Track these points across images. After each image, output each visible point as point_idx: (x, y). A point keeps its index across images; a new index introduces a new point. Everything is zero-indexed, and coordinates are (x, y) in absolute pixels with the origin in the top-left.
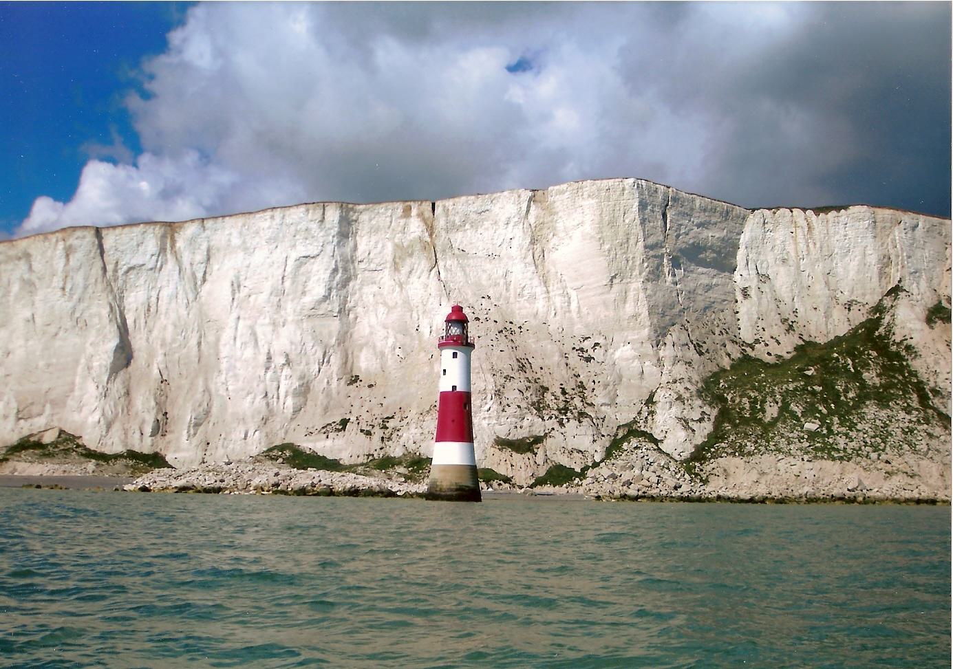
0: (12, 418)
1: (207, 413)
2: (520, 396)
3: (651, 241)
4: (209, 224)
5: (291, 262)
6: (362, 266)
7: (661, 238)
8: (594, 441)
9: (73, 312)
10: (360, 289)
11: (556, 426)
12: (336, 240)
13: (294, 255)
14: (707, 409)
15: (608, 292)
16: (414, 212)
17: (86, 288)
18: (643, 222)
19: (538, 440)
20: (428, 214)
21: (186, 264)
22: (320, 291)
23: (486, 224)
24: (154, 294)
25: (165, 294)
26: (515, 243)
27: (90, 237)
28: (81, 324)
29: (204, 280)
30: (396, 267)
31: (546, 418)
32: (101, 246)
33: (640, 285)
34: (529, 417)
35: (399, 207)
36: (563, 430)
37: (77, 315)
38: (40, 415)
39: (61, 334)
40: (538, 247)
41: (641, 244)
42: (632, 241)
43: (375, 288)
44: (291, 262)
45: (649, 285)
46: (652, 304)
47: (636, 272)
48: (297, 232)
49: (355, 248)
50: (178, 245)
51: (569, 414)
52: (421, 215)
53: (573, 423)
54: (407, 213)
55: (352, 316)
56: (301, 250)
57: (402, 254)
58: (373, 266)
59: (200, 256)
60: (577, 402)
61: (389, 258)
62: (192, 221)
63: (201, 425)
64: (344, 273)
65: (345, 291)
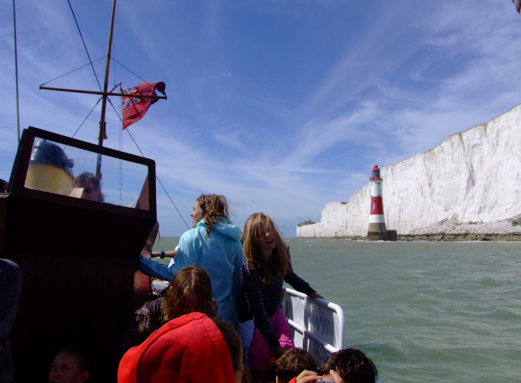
0: (444, 211)
1: (496, 203)
4: (496, 120)
17: (459, 157)
21: (490, 140)
24: (481, 155)
25: (485, 153)
27: (457, 137)
28: (458, 172)
29: (497, 145)
32: (461, 139)
38: (450, 209)
39: (454, 177)
50: (488, 132)
62: (490, 120)
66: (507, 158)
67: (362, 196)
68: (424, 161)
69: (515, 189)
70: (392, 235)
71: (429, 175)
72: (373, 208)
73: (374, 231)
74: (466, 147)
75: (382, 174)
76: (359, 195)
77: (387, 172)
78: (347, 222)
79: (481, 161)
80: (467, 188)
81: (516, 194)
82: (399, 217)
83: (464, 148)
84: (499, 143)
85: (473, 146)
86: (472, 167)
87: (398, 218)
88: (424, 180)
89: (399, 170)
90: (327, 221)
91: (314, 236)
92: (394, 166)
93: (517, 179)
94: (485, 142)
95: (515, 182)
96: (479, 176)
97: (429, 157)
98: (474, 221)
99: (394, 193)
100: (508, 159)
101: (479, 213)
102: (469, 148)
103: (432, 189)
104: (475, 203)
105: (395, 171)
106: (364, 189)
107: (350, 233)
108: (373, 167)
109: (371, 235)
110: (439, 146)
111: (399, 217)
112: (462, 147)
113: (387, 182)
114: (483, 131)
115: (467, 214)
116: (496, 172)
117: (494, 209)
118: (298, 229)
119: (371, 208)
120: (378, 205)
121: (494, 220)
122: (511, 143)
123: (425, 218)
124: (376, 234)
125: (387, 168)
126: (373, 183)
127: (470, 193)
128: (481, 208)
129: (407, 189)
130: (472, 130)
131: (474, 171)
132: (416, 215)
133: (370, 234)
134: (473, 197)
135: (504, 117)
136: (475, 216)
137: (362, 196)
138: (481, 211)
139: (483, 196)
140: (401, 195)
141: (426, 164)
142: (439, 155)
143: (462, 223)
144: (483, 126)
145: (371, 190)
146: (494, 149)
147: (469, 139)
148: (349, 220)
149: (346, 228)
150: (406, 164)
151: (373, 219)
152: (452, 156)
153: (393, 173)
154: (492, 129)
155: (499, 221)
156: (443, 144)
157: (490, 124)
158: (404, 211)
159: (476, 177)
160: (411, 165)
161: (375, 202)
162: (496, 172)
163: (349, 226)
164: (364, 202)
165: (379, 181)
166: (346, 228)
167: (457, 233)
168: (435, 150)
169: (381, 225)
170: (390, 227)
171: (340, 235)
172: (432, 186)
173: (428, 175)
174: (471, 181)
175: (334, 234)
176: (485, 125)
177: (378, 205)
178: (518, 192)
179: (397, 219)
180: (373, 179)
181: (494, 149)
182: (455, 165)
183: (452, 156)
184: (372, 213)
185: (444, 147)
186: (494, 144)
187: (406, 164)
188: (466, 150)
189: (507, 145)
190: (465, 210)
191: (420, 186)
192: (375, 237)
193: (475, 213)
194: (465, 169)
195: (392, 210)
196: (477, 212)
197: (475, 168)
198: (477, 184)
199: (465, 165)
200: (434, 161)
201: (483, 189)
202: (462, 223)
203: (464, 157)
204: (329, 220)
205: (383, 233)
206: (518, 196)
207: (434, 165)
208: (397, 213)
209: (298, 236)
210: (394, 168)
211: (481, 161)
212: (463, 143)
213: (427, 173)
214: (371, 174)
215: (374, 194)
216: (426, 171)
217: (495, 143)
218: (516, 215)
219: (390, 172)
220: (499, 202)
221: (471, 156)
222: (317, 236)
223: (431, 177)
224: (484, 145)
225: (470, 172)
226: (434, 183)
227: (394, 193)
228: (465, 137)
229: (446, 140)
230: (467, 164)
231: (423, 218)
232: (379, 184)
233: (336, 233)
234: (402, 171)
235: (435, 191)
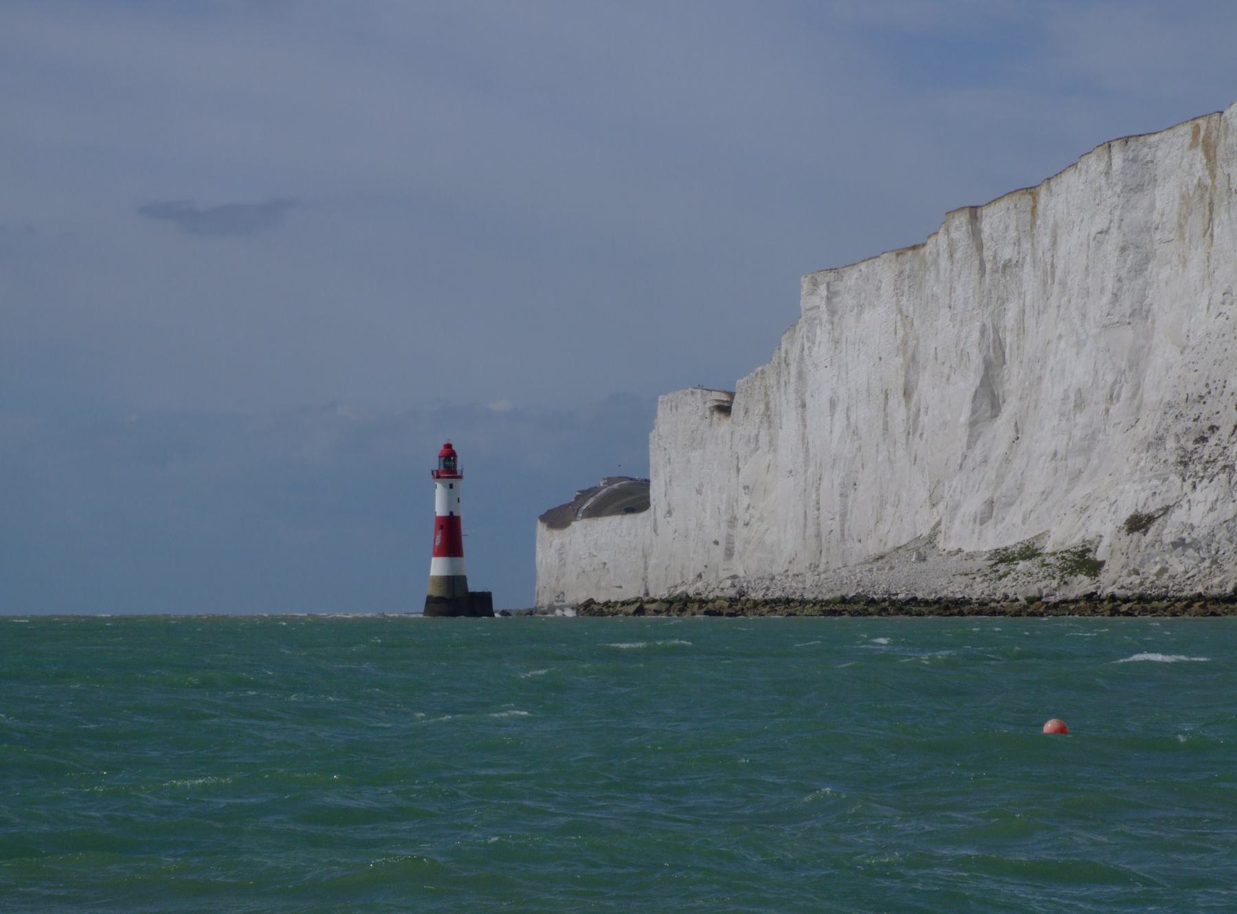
9: (957, 345)
27: (962, 219)
32: (976, 234)
35: (1188, 128)
49: (1152, 208)
63: (1011, 505)
65: (1141, 281)
70: (480, 604)
72: (437, 543)
74: (989, 266)
78: (732, 522)
79: (1021, 329)
80: (973, 424)
82: (844, 516)
86: (999, 345)
99: (833, 404)
103: (913, 409)
108: (442, 448)
111: (844, 516)
112: (977, 263)
113: (816, 349)
114: (1028, 217)
118: (550, 547)
127: (979, 443)
128: (991, 503)
131: (1004, 363)
133: (431, 601)
138: (991, 517)
141: (904, 300)
144: (1029, 197)
149: (729, 553)
151: (438, 567)
153: (833, 312)
159: (1007, 386)
161: (442, 528)
170: (474, 586)
172: (915, 398)
177: (450, 536)
180: (438, 477)
188: (987, 277)
193: (975, 521)
205: (459, 600)
209: (544, 600)
210: (839, 286)
212: (980, 247)
213: (905, 343)
214: (435, 464)
215: (440, 510)
216: (901, 333)
230: (983, 331)
232: (451, 486)
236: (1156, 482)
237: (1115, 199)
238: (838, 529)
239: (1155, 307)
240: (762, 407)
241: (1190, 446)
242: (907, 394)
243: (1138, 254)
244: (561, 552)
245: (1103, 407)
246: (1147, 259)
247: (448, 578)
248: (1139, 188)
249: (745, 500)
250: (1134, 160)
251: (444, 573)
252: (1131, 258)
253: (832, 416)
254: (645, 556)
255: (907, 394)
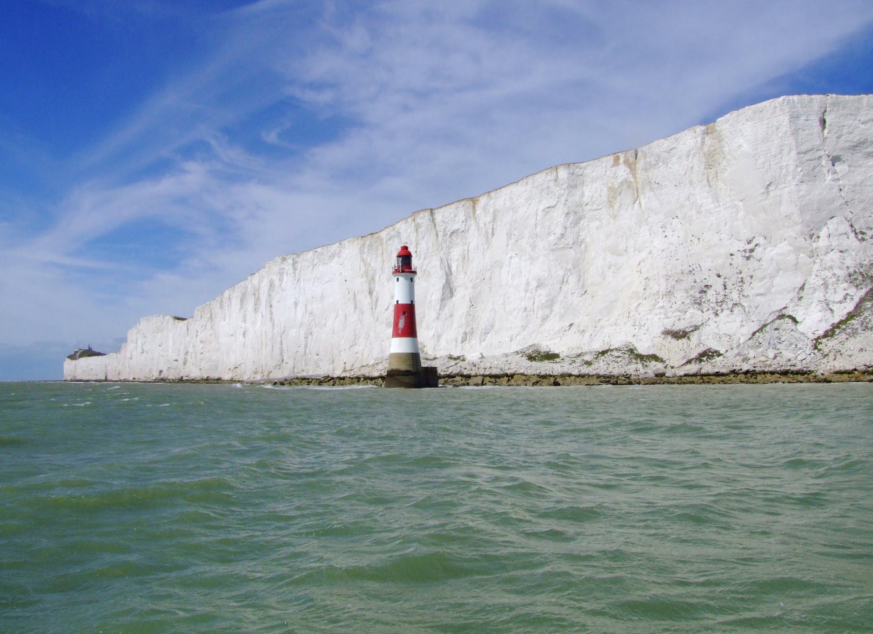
1: (492, 326)
2: (685, 295)
3: (804, 148)
4: (493, 194)
5: (540, 213)
6: (588, 207)
7: (818, 142)
8: (742, 326)
10: (588, 225)
11: (712, 316)
12: (567, 192)
13: (542, 207)
14: (852, 291)
15: (766, 199)
16: (622, 160)
17: (428, 249)
18: (795, 132)
19: (696, 328)
20: (631, 159)
21: (482, 225)
22: (559, 231)
23: (674, 159)
24: (466, 248)
25: (472, 246)
26: (696, 167)
27: (427, 214)
29: (493, 235)
30: (610, 204)
31: (705, 310)
32: (433, 220)
33: (793, 188)
34: (691, 311)
35: (611, 158)
36: (717, 319)
37: (424, 267)
40: (713, 171)
41: (793, 153)
42: (785, 152)
43: (597, 223)
44: (540, 213)
45: (804, 187)
46: (804, 203)
47: (790, 178)
48: (542, 190)
49: (583, 195)
51: (724, 305)
52: (626, 162)
53: (727, 312)
54: (616, 161)
55: (583, 246)
56: (546, 203)
57: (614, 193)
58: (595, 207)
59: (489, 219)
60: (735, 296)
61: (605, 199)
64: (576, 215)
66: (509, 256)
67: (221, 307)
68: (361, 252)
69: (523, 305)
71: (370, 277)
72: (401, 325)
73: (403, 367)
74: (440, 234)
75: (415, 262)
76: (215, 305)
77: (283, 266)
78: (187, 353)
79: (465, 258)
80: (443, 300)
81: (525, 314)
82: (306, 346)
83: (437, 235)
84: (496, 232)
85: (452, 233)
86: (449, 267)
87: (303, 346)
88: (359, 284)
89: (307, 264)
90: (140, 350)
91: (104, 378)
92: (298, 255)
93: (527, 291)
94: (472, 228)
95: (523, 294)
96: (460, 281)
97: (371, 245)
98: (455, 355)
99: (296, 304)
100: (511, 258)
101: (462, 342)
102: (445, 235)
103: (374, 299)
104: (455, 325)
105: (299, 266)
106: (226, 294)
107: (194, 373)
109: (393, 377)
110: (391, 228)
111: (306, 346)
113: (283, 284)
115: (443, 342)
116: (491, 277)
117: (489, 335)
119: (396, 324)
120: (406, 319)
121: (498, 352)
122: (516, 232)
123: (361, 348)
124: (406, 373)
125: (284, 259)
126: (401, 278)
128: (466, 334)
129: (322, 298)
130: (453, 206)
132: (343, 342)
134: (451, 316)
135: (506, 191)
136: (456, 346)
137: (221, 307)
139: (468, 314)
140: (309, 308)
141: (365, 256)
142: (390, 242)
143: (435, 358)
145: (396, 291)
146: (487, 240)
147: (446, 220)
148: (191, 350)
149: (185, 363)
150: (322, 254)
151: (400, 346)
152: (416, 247)
153: (295, 269)
154: (484, 208)
155: (507, 355)
156: (398, 226)
157: (483, 200)
158: (315, 335)
159: (455, 284)
160: (332, 257)
162: (491, 277)
163: (190, 361)
164: (227, 318)
165: (411, 275)
166: (185, 363)
167: (487, 373)
168: (383, 234)
169: (415, 357)
171: (171, 377)
172: (374, 294)
173: (367, 276)
174: (449, 290)
175: (155, 375)
176: (474, 200)
177: (406, 319)
178: (528, 309)
179: (302, 349)
180: (403, 271)
181: (487, 240)
182: (421, 261)
183: (416, 247)
184: (397, 334)
185: (402, 231)
186: (487, 232)
187: (322, 254)
188: (440, 238)
189: (509, 235)
190: (439, 337)
191: (351, 295)
192: (407, 379)
194: (438, 269)
195: (293, 332)
196: (460, 339)
197: (454, 269)
198: (459, 294)
199: (438, 263)
200: (380, 252)
201: (468, 304)
202: (435, 358)
203: (437, 250)
204: (146, 348)
206: (527, 316)
207: (380, 259)
208: (302, 339)
209: (69, 378)
210: (299, 260)
211: (465, 258)
212: (435, 226)
213: (366, 272)
214: (394, 261)
215: (403, 301)
217: (490, 231)
218: (526, 346)
219: (290, 267)
220: (497, 326)
221: (449, 248)
222: (109, 378)
223: (373, 278)
224: (471, 232)
225: (447, 275)
226: (377, 288)
227: (296, 304)
228: (439, 216)
229: (406, 219)
230: (442, 260)
231: (356, 348)
232: (412, 280)
233: (161, 372)
234: (314, 266)
235: (379, 303)
236: (679, 313)
237: (563, 192)
238: (303, 350)
239: (588, 240)
240: (209, 315)
241: (698, 295)
242: (370, 293)
243: (576, 215)
244: (75, 366)
245: (558, 286)
246: (580, 219)
247: (412, 354)
248: (575, 187)
249: (202, 346)
250: (573, 174)
251: (410, 351)
252: (572, 218)
253: (296, 308)
254: (106, 366)
255: (370, 293)
